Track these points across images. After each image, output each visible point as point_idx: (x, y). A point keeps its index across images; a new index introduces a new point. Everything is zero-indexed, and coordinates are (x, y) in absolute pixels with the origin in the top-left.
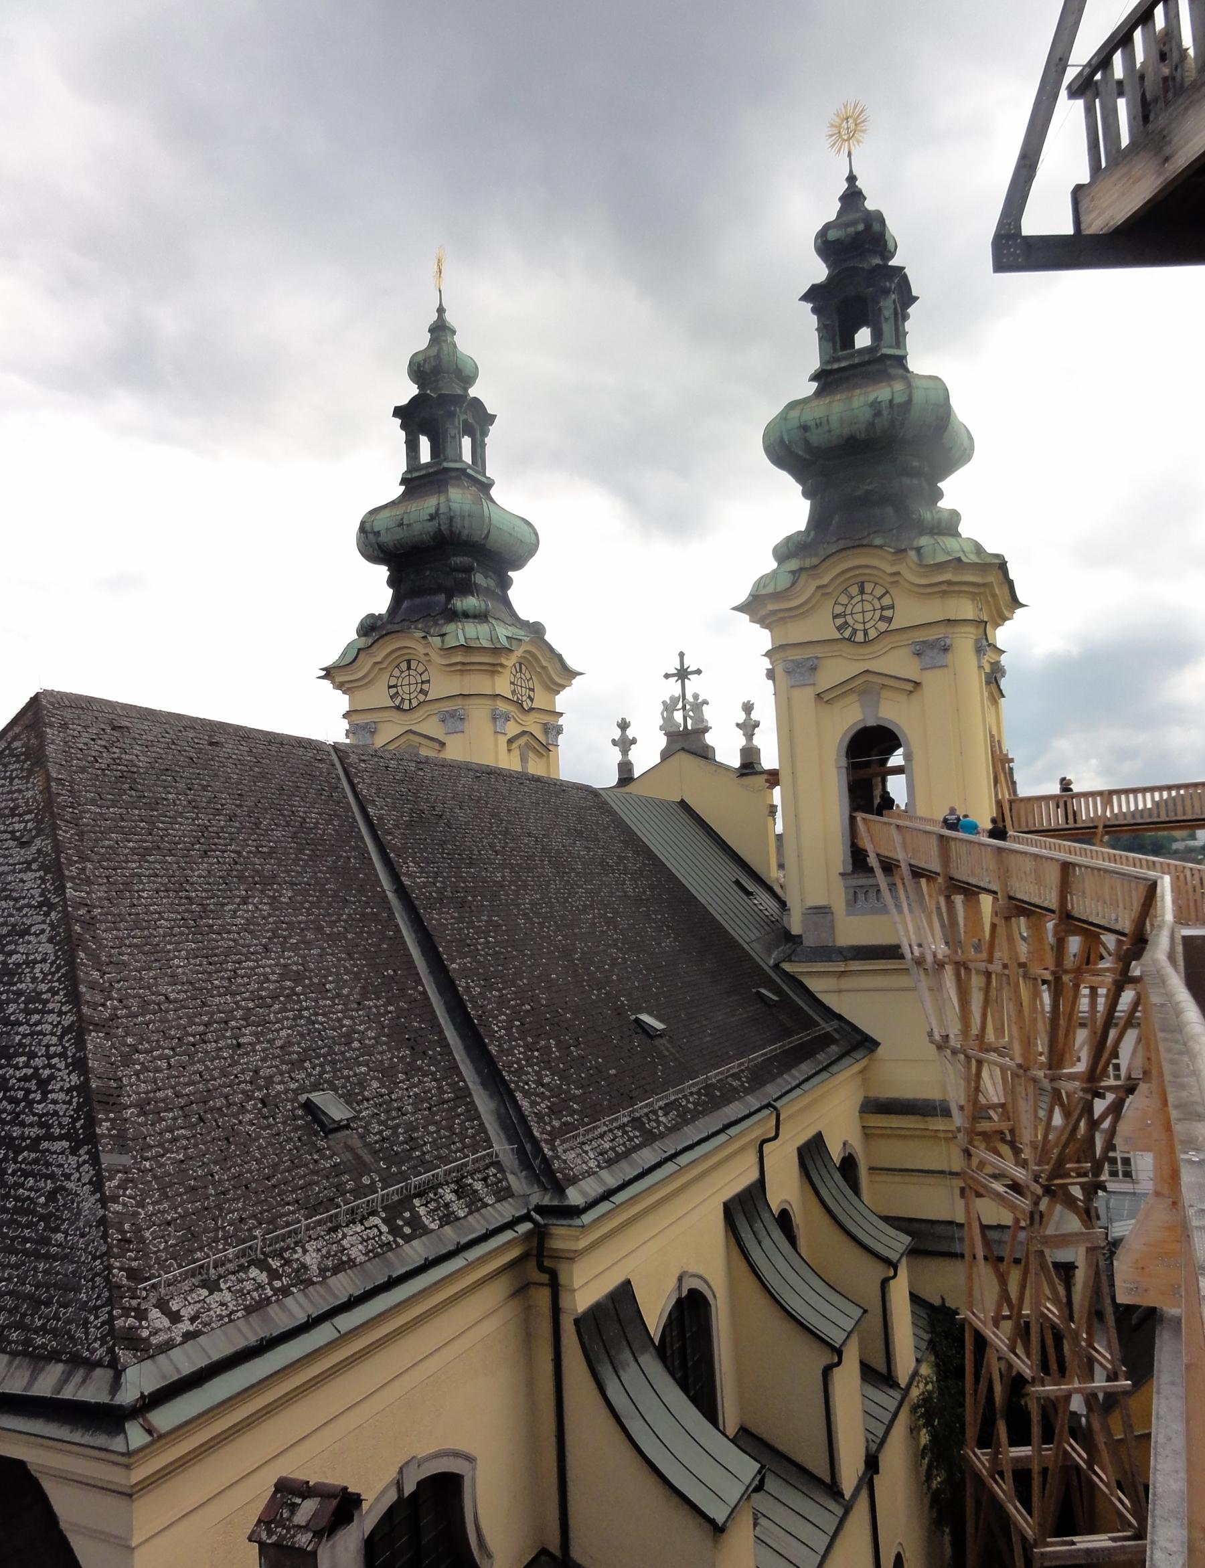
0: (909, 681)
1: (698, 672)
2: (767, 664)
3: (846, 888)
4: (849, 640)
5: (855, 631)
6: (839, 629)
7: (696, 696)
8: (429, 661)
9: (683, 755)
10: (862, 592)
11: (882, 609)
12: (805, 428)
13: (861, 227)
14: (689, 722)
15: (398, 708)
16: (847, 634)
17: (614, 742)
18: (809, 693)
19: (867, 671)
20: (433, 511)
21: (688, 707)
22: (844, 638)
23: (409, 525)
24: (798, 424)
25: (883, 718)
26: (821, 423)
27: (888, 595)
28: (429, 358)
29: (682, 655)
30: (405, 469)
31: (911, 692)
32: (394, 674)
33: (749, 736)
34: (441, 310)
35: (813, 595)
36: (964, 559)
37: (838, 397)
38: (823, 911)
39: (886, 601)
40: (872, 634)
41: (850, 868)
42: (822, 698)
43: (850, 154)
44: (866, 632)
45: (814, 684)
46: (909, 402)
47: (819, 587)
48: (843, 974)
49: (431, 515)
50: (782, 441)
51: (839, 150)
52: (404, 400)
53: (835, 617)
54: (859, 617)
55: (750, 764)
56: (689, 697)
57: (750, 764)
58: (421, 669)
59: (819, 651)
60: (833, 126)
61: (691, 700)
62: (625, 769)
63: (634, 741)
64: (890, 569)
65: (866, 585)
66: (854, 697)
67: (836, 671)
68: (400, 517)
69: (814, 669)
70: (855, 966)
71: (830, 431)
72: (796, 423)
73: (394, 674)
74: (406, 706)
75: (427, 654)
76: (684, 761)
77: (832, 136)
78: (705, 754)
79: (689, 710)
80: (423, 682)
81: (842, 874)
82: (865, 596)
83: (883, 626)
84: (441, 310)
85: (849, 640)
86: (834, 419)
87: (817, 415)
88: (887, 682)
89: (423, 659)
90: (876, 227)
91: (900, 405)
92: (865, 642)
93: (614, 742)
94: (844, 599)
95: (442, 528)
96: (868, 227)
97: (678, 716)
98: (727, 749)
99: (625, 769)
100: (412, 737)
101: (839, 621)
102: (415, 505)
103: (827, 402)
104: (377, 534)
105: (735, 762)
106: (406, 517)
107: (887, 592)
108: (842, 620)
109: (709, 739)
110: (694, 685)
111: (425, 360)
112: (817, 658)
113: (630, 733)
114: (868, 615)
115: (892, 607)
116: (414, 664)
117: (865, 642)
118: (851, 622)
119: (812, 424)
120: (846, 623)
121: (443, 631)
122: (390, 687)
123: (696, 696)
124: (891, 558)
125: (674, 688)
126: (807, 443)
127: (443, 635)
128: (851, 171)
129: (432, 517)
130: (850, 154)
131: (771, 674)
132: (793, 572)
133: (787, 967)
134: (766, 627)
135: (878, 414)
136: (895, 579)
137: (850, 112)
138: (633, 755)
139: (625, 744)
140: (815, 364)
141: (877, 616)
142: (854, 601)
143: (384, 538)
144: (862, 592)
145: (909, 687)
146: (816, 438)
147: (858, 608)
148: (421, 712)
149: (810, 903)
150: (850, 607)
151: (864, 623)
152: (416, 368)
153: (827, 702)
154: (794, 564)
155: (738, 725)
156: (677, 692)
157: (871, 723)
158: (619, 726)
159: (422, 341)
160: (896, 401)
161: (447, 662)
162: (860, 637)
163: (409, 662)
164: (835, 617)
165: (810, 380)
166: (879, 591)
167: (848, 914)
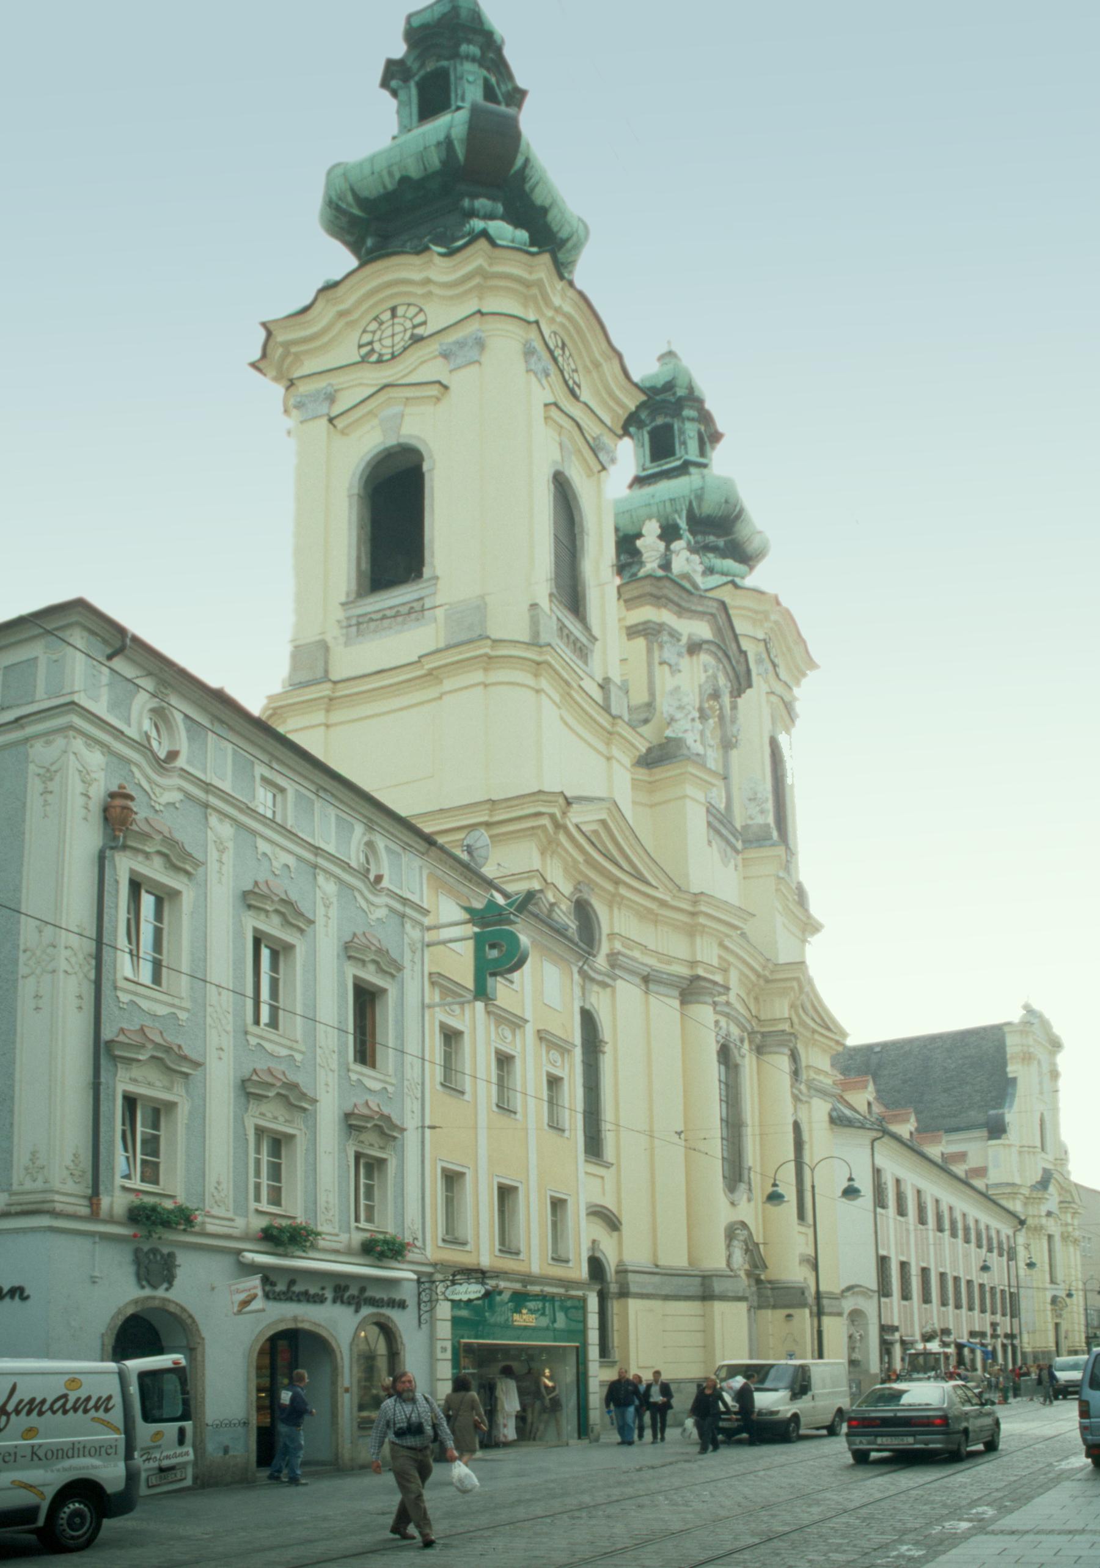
10: (394, 315)
31: (438, 399)
47: (341, 314)
94: (374, 326)
101: (364, 351)
108: (369, 348)
120: (373, 351)
142: (383, 327)
144: (394, 315)
145: (434, 391)
150: (379, 333)
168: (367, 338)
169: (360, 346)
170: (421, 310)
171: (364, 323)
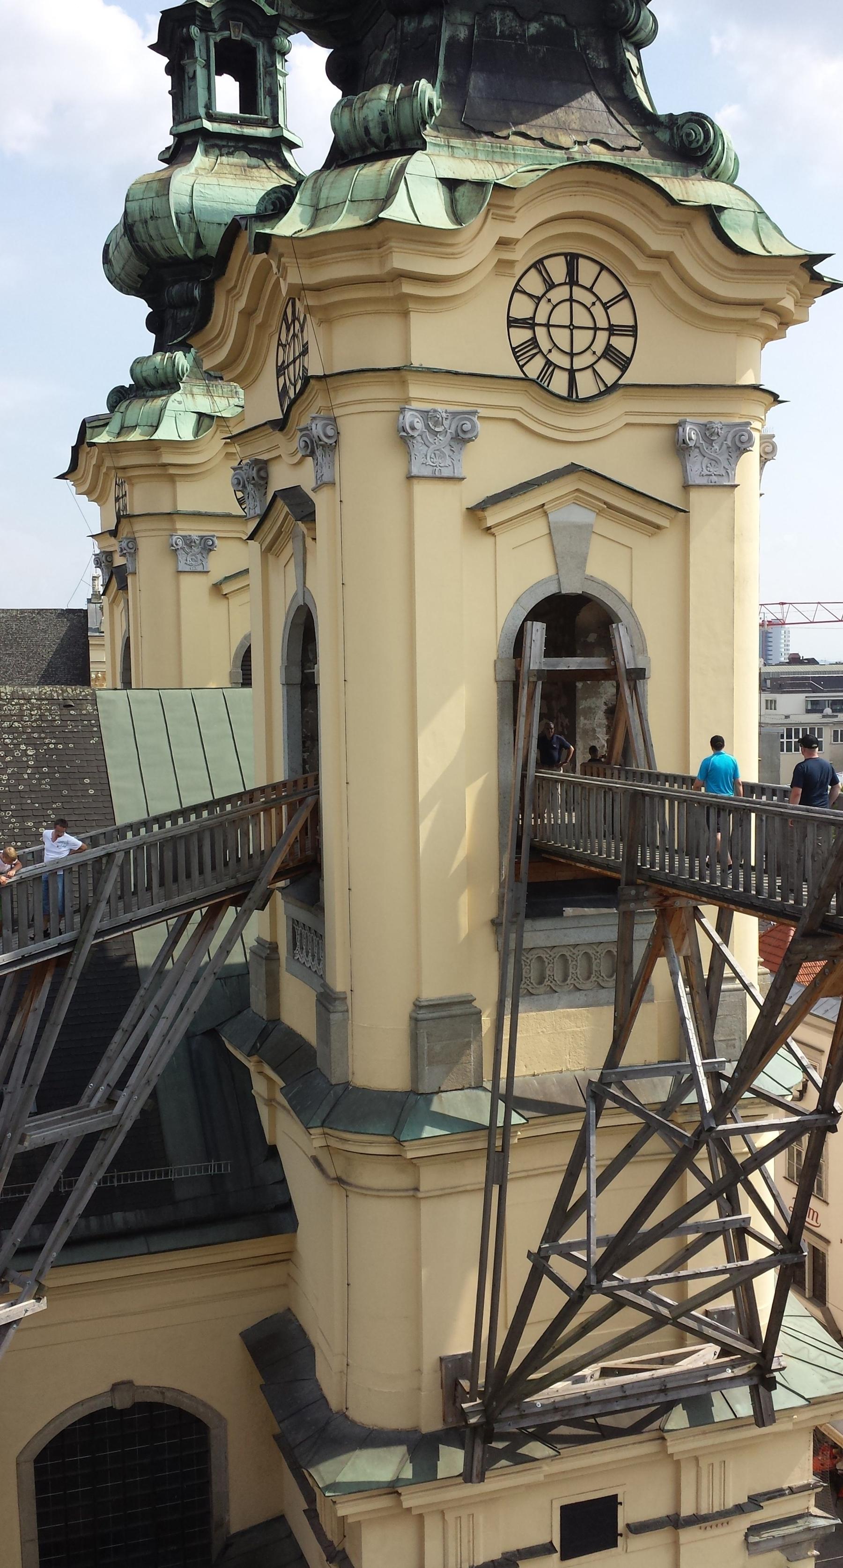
11: (612, 330)
22: (526, 379)
40: (586, 385)
65: (582, 263)
83: (609, 372)
92: (568, 399)
94: (534, 284)
101: (521, 335)
115: (633, 330)
120: (534, 341)
141: (599, 346)
144: (572, 280)
147: (561, 316)
162: (559, 383)
168: (523, 308)
169: (512, 323)
170: (625, 295)
171: (519, 271)
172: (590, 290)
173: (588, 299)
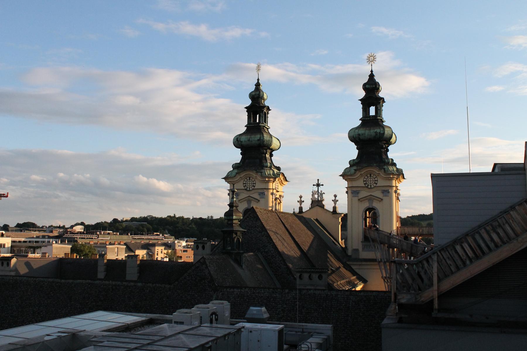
0: (380, 198)
1: (323, 185)
2: (346, 190)
3: (362, 245)
4: (367, 187)
5: (368, 185)
6: (365, 184)
7: (321, 191)
8: (256, 178)
9: (318, 207)
10: (371, 176)
12: (359, 135)
13: (374, 86)
14: (319, 198)
15: (246, 190)
16: (366, 186)
17: (298, 201)
18: (356, 199)
19: (371, 195)
20: (259, 138)
21: (319, 194)
23: (251, 141)
24: (358, 134)
25: (374, 206)
26: (363, 134)
27: (376, 178)
28: (256, 94)
29: (318, 180)
30: (247, 124)
32: (245, 180)
33: (335, 204)
34: (258, 80)
35: (359, 176)
36: (395, 173)
37: (367, 129)
38: (356, 251)
39: (376, 179)
40: (372, 186)
41: (363, 240)
42: (360, 200)
43: (372, 65)
44: (371, 186)
45: (358, 197)
46: (384, 133)
47: (361, 174)
48: (360, 265)
49: (258, 139)
50: (353, 137)
51: (369, 63)
52: (248, 105)
53: (364, 181)
54: (369, 182)
55: (335, 211)
56: (320, 191)
57: (335, 211)
58: (253, 180)
59: (359, 189)
60: (368, 57)
61: (320, 192)
62: (301, 208)
63: (303, 201)
64: (377, 172)
65: (372, 175)
66: (367, 201)
67: (364, 194)
68: (248, 139)
69: (358, 193)
70: (364, 263)
71: (365, 137)
72: (357, 133)
73: (245, 180)
74: (248, 189)
75: (256, 177)
76: (318, 209)
77: (368, 59)
78: (323, 206)
79: (319, 195)
80: (253, 184)
81: (362, 242)
82: (371, 177)
83: (375, 185)
84: (258, 80)
85: (367, 187)
86: (366, 134)
87: (363, 132)
88: (375, 198)
89: (255, 178)
90: (378, 86)
91: (382, 134)
92: (370, 188)
93: (298, 201)
94: (366, 177)
95: (261, 143)
96: (376, 86)
97: (316, 196)
98: (328, 205)
99: (301, 208)
100: (250, 198)
102: (253, 136)
103: (365, 129)
104: (242, 142)
105: (332, 210)
106: (250, 139)
107: (376, 177)
109: (324, 203)
110: (321, 188)
111: (255, 95)
112: (359, 190)
113: (302, 199)
114: (372, 182)
115: (377, 181)
116: (251, 179)
117: (370, 188)
118: (367, 183)
119: (361, 134)
121: (261, 171)
122: (243, 184)
123: (321, 191)
124: (378, 170)
125: (315, 188)
126: (359, 138)
127: (261, 172)
128: (372, 69)
129: (258, 140)
130: (372, 65)
131: (347, 192)
132: (355, 170)
133: (348, 263)
134: (346, 180)
135: (376, 135)
136: (379, 174)
137: (372, 55)
138: (303, 205)
139: (301, 202)
140: (361, 116)
141: (374, 183)
142: (369, 178)
143: (243, 143)
145: (380, 200)
146: (361, 137)
147: (369, 180)
148: (253, 191)
149: (354, 248)
150: (368, 179)
151: (371, 184)
152: (252, 96)
153: (361, 201)
154: (355, 168)
155: (333, 200)
156: (316, 190)
157: (371, 207)
158: (300, 197)
159: (253, 88)
160: (381, 132)
161: (262, 180)
162: (369, 187)
163: (250, 178)
164: (364, 181)
165: (360, 120)
166: (374, 177)
167: (362, 251)
172: (373, 177)
173: (372, 178)
